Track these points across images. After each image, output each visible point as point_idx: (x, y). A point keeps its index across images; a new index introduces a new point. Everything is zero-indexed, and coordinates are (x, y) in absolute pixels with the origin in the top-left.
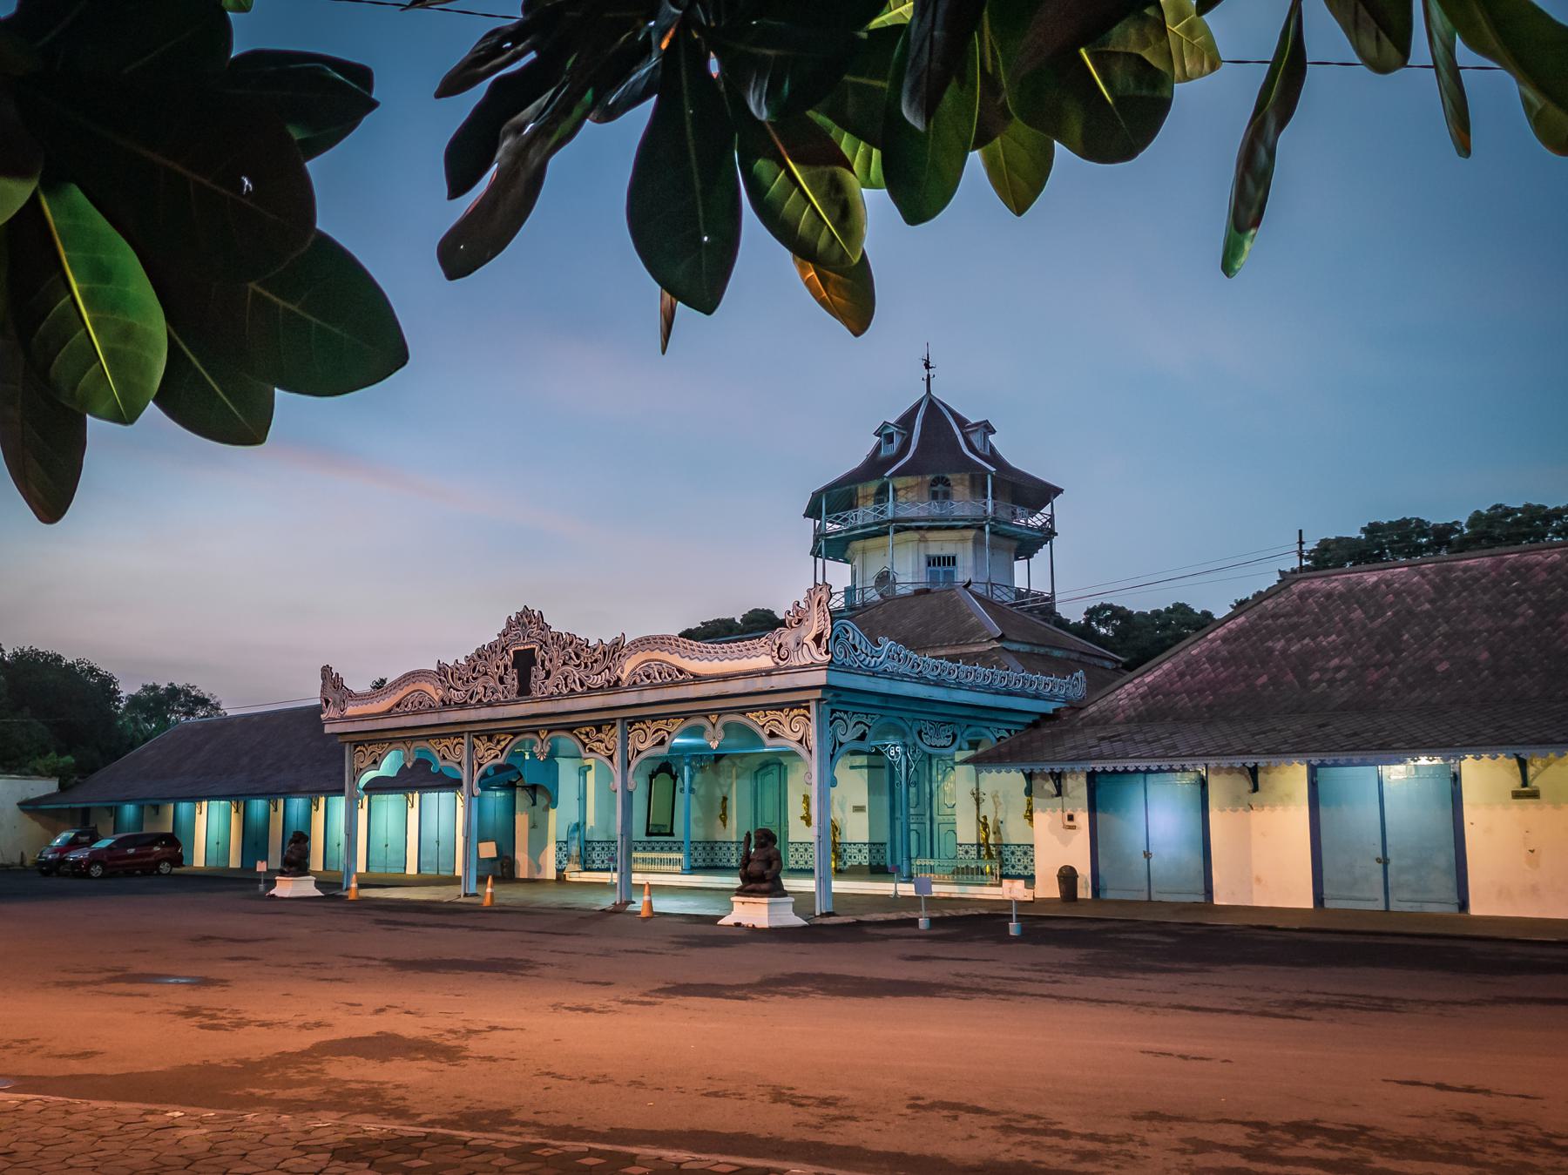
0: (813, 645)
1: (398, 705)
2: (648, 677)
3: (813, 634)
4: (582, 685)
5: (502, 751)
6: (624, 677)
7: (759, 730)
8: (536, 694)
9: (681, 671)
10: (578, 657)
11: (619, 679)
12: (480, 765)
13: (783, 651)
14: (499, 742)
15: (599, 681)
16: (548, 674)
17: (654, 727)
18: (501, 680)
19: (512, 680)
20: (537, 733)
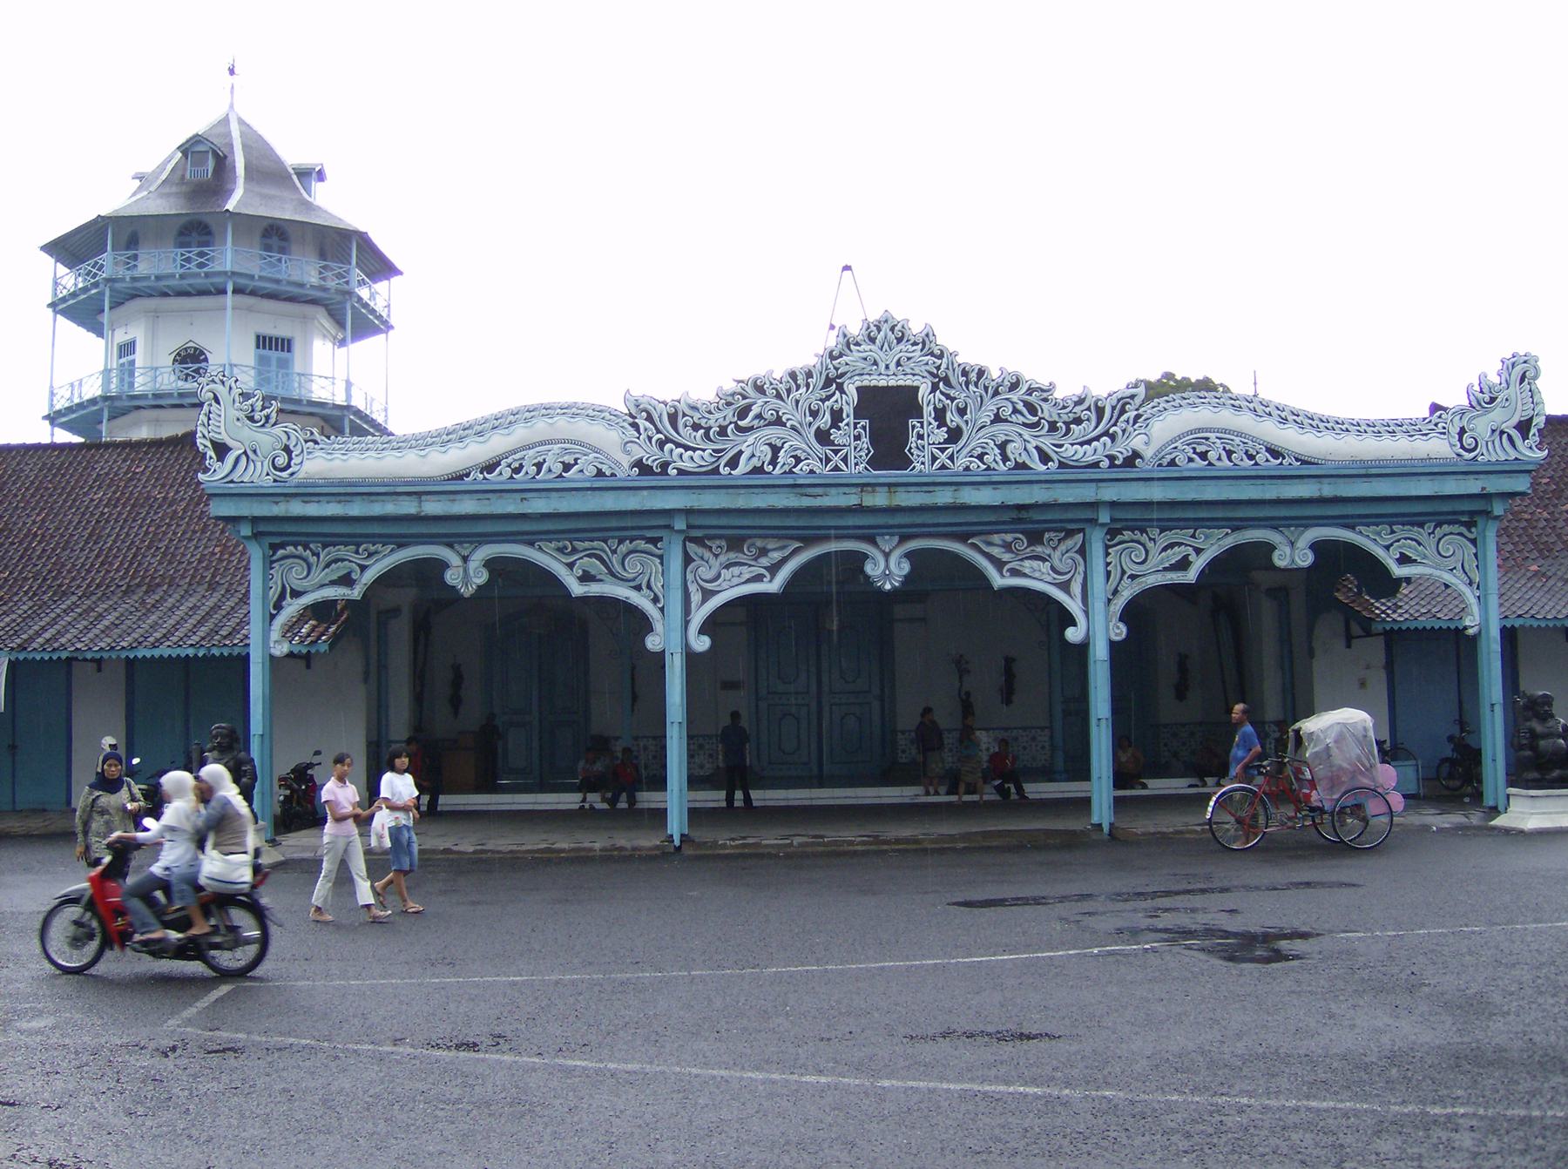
0: (1515, 434)
1: (490, 467)
2: (1203, 456)
3: (1515, 420)
4: (1045, 458)
5: (774, 569)
6: (1148, 453)
7: (1379, 553)
8: (921, 465)
9: (1275, 453)
10: (1032, 409)
11: (1136, 455)
12: (707, 595)
13: (1468, 441)
14: (764, 552)
15: (1087, 454)
16: (955, 435)
17: (1163, 540)
18: (823, 437)
19: (854, 442)
20: (871, 540)
